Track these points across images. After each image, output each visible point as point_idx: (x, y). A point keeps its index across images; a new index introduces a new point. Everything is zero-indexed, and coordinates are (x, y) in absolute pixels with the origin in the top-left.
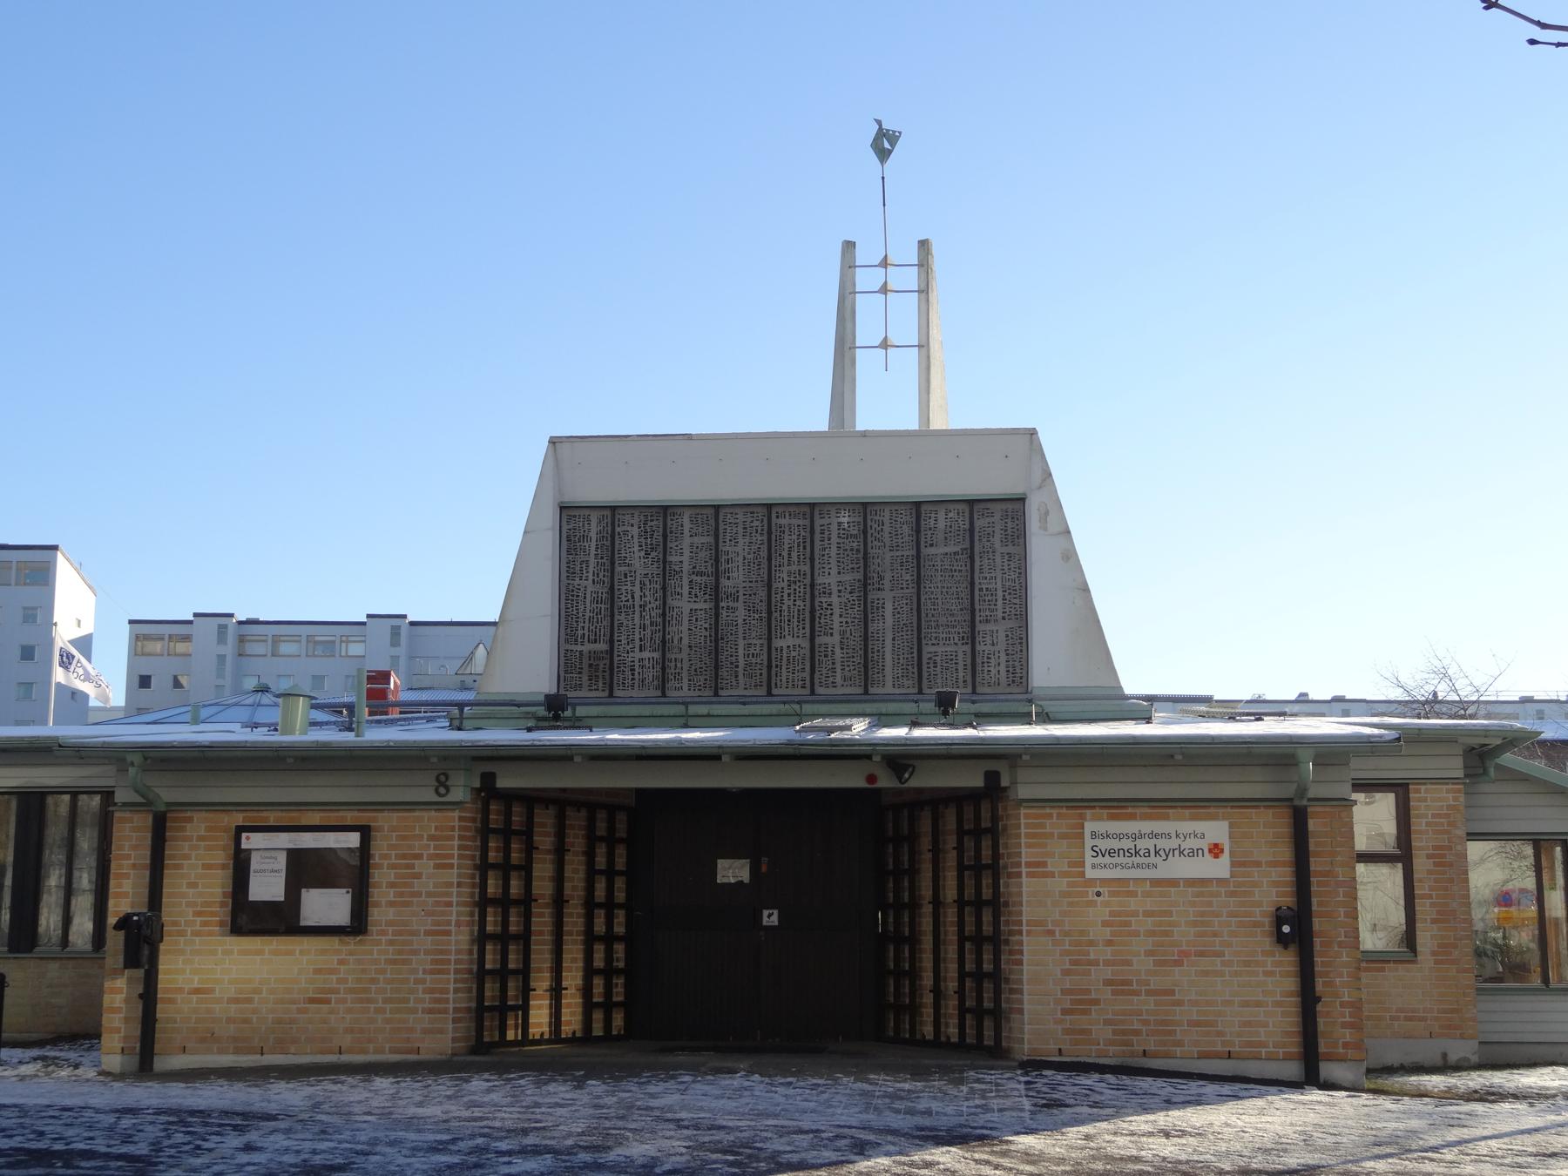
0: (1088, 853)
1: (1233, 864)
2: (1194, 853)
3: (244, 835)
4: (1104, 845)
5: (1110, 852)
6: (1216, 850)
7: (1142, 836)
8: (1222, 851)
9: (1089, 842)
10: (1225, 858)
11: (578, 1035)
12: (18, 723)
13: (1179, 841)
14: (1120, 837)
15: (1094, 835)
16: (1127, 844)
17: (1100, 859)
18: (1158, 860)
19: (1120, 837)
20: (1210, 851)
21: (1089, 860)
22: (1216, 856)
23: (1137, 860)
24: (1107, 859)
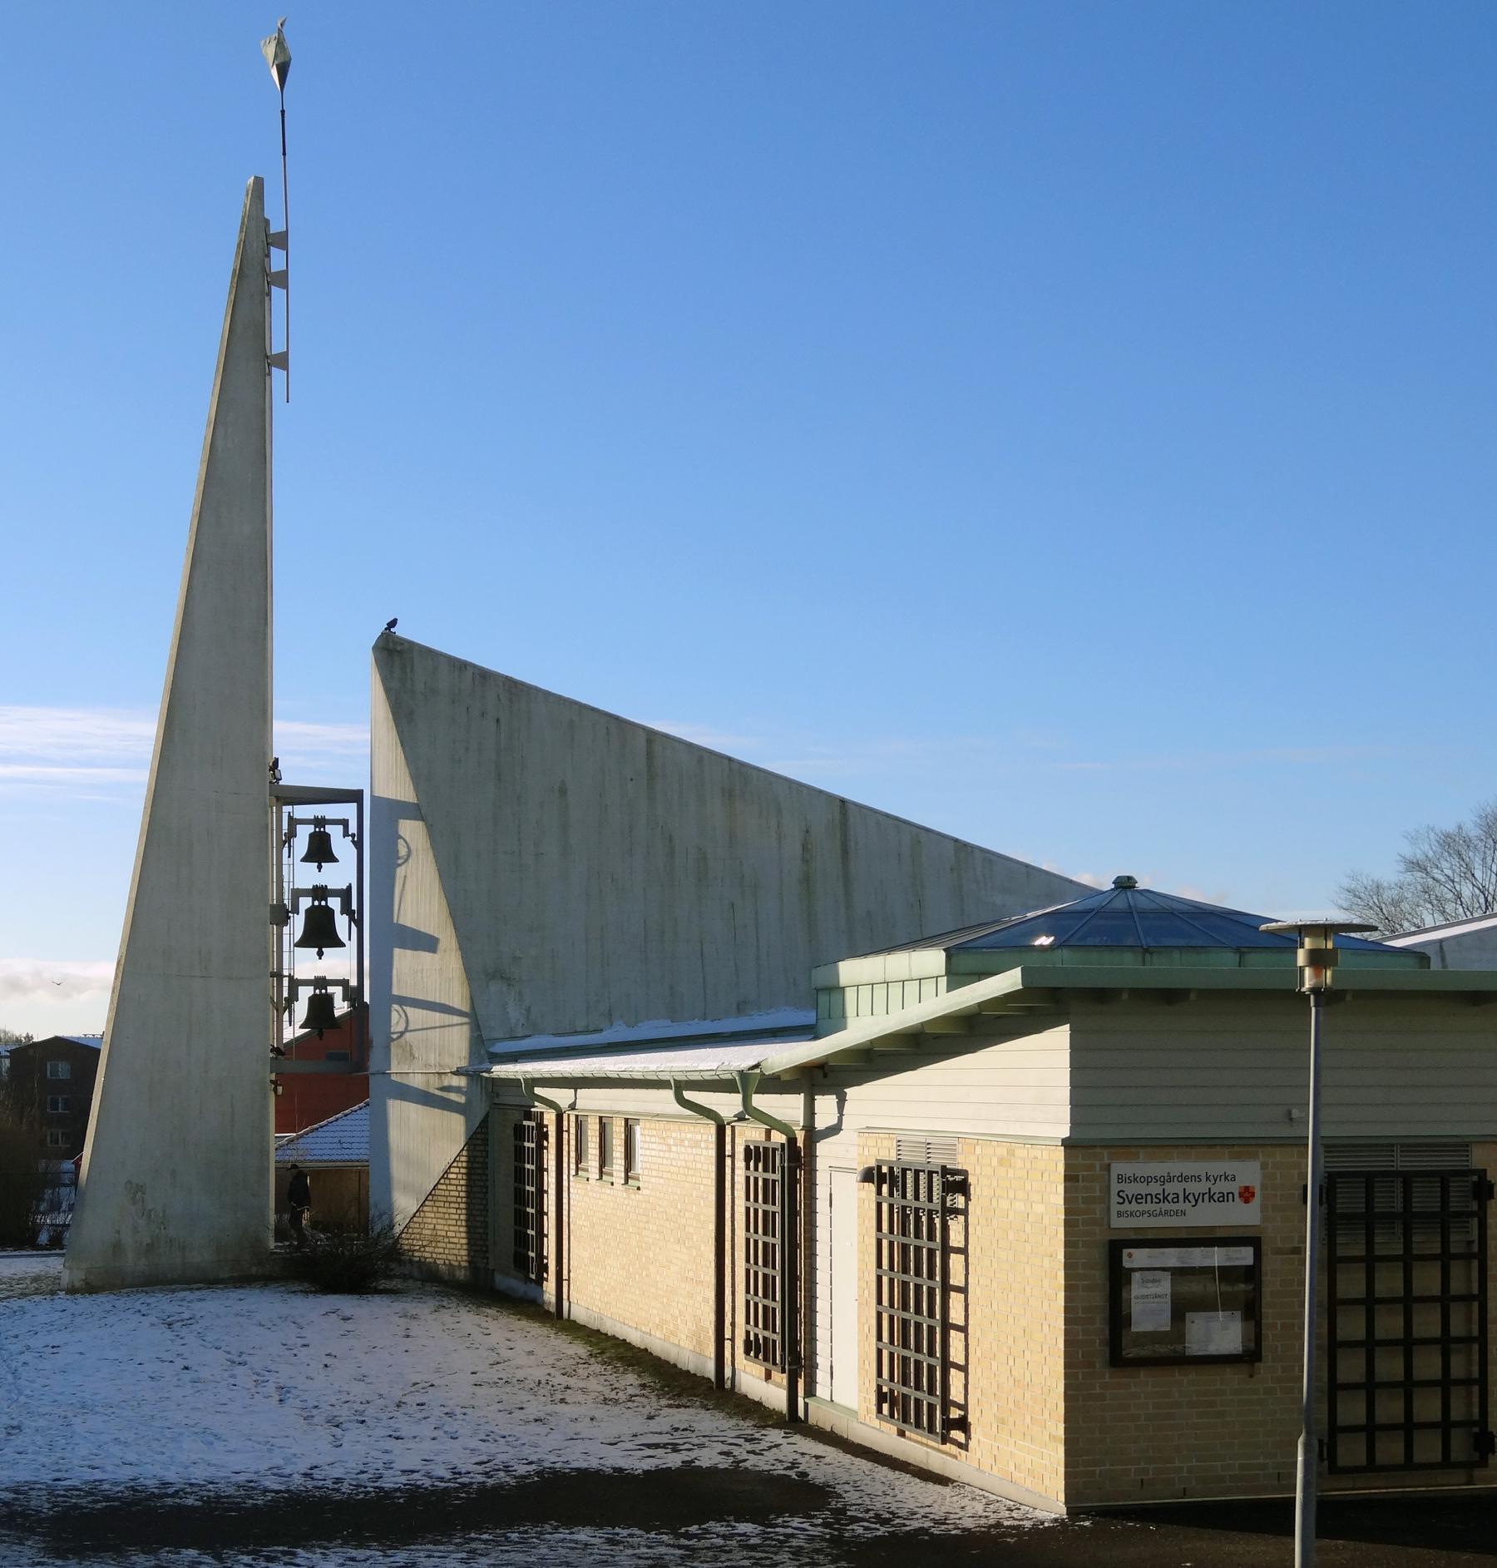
0: (1115, 1199)
1: (1264, 1208)
2: (1224, 1197)
3: (1125, 1252)
4: (1131, 1189)
5: (1138, 1198)
6: (1247, 1195)
7: (1170, 1179)
8: (1253, 1195)
9: (1115, 1187)
10: (1256, 1201)
11: (461, 1275)
12: (1305, 1202)
13: (1209, 1184)
14: (1147, 1180)
15: (1120, 1179)
16: (1155, 1188)
17: (1127, 1207)
18: (1187, 1206)
19: (1147, 1180)
20: (1241, 1195)
21: (1115, 1208)
22: (1247, 1201)
23: (1166, 1206)
24: (1134, 1207)
